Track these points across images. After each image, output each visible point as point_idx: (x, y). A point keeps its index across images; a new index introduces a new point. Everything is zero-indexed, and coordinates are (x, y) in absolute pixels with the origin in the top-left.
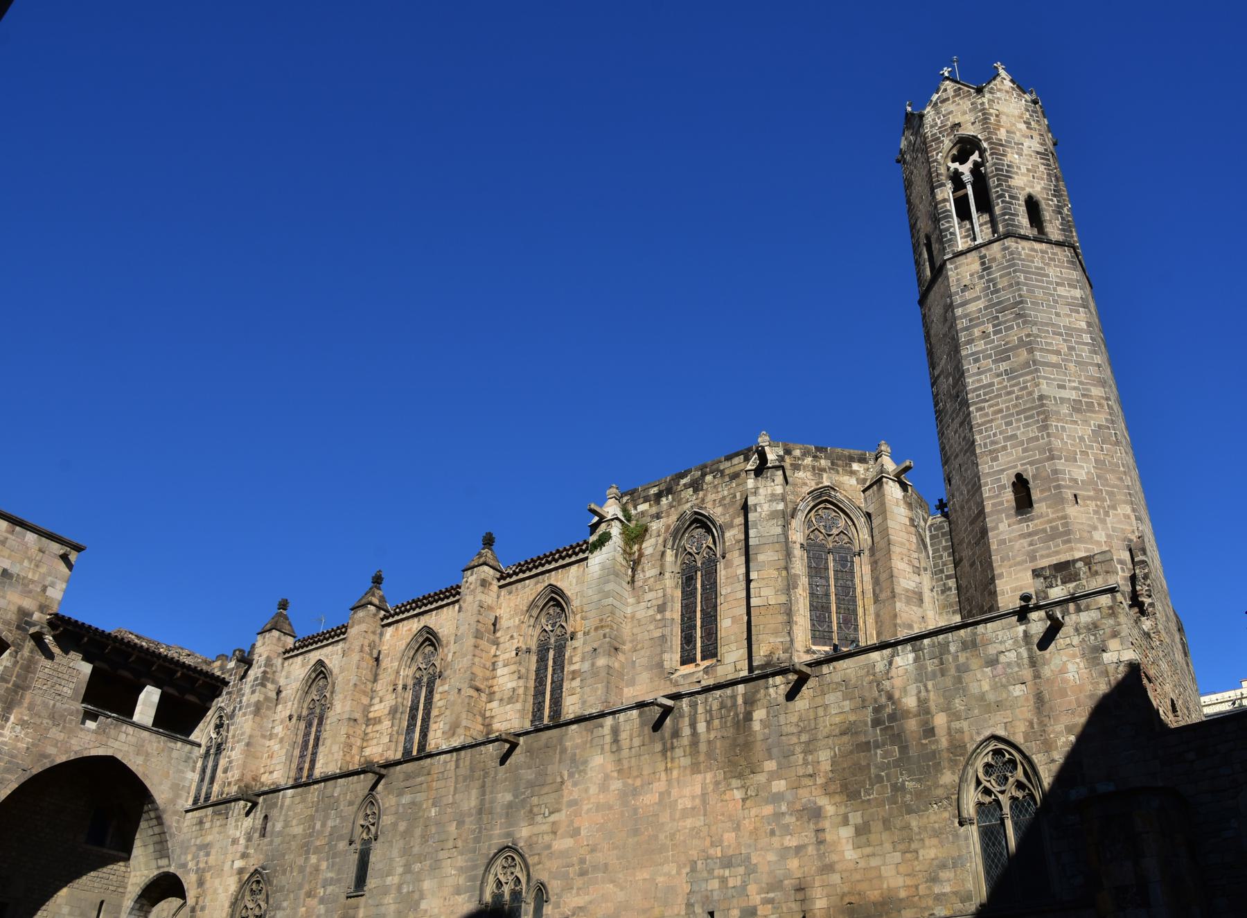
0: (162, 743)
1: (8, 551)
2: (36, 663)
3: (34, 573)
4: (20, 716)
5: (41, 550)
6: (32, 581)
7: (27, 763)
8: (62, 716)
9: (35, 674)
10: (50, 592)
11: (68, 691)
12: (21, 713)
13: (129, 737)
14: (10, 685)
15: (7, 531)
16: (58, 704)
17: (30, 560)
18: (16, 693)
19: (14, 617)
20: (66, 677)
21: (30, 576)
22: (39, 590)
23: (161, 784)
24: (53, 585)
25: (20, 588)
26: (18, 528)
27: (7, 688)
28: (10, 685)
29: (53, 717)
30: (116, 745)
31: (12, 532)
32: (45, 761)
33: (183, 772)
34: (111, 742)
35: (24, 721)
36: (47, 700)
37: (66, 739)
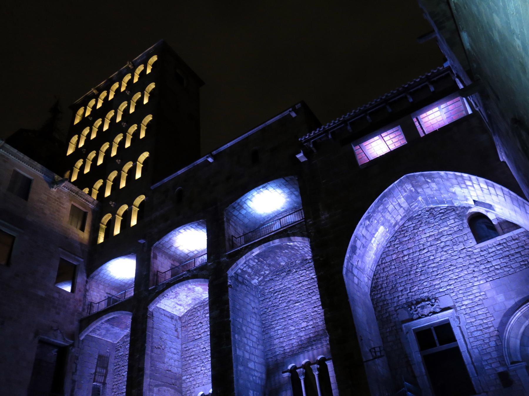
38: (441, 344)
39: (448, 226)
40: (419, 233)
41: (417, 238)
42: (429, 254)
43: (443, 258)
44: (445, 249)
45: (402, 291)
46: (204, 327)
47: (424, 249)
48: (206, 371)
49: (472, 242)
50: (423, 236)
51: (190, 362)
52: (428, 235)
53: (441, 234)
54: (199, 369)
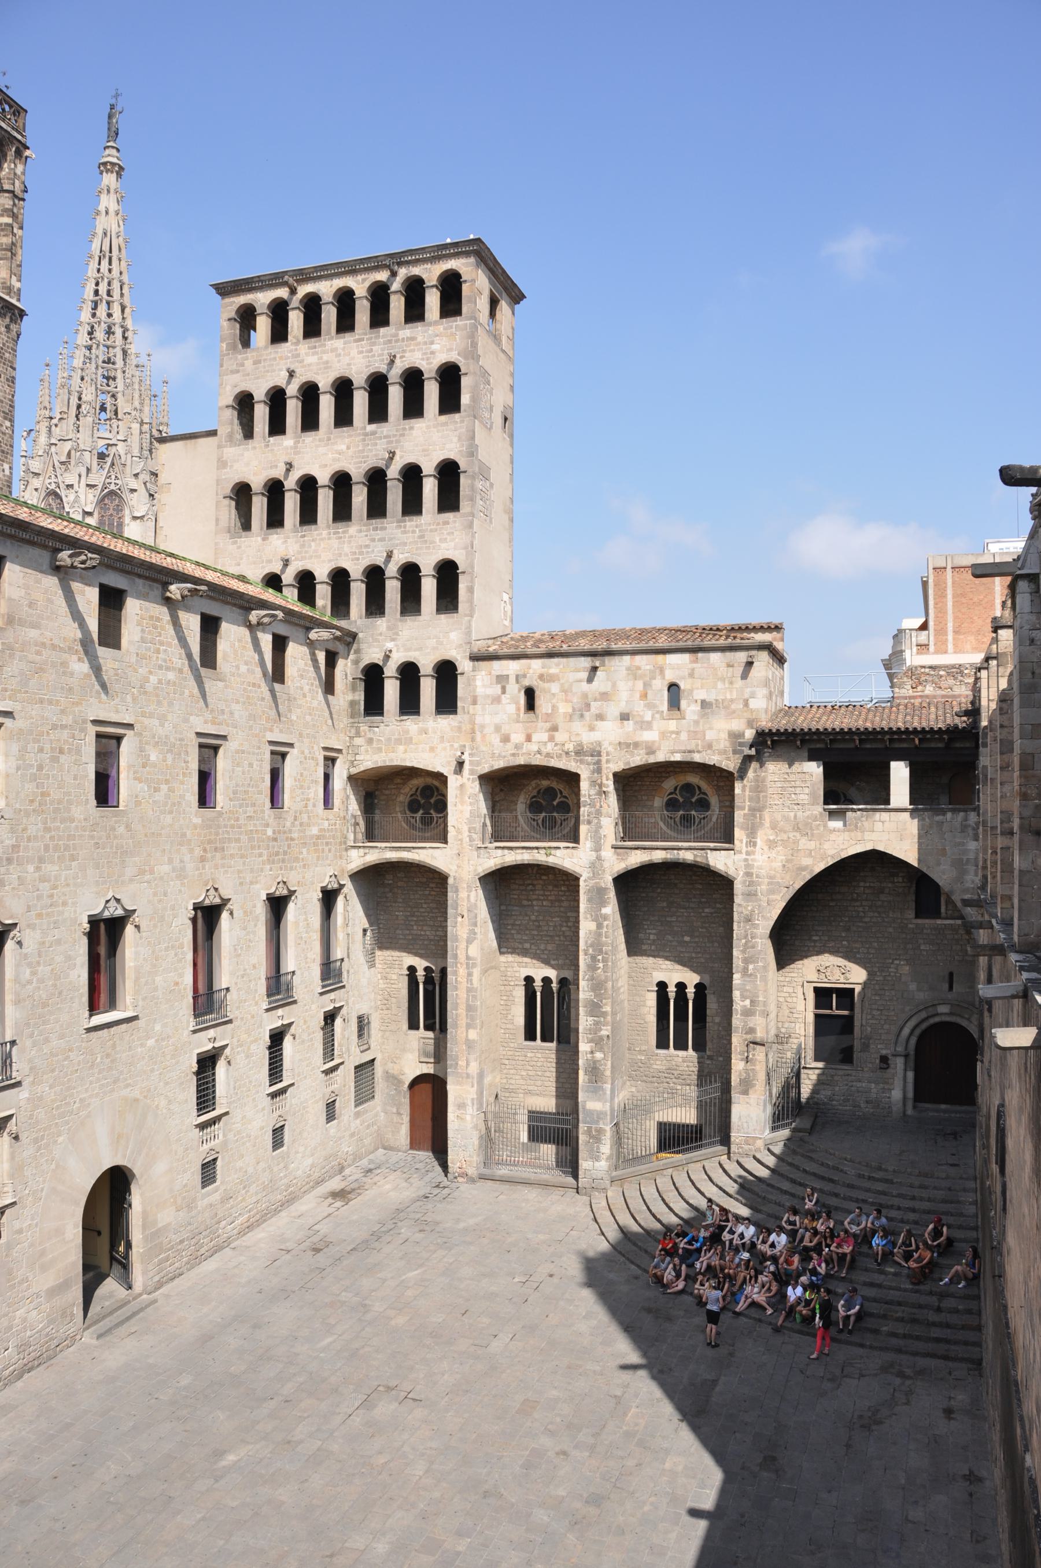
0: (927, 820)
1: (700, 680)
2: (763, 781)
3: (731, 692)
4: (766, 838)
5: (729, 666)
6: (732, 701)
7: (788, 880)
8: (806, 824)
9: (766, 792)
10: (753, 704)
11: (804, 798)
12: (766, 834)
13: (886, 824)
14: (746, 811)
15: (692, 662)
16: (800, 814)
17: (723, 680)
18: (754, 816)
19: (727, 744)
20: (798, 783)
21: (729, 697)
22: (742, 706)
23: (939, 864)
24: (753, 695)
25: (723, 712)
26: (700, 655)
27: (745, 815)
28: (746, 811)
29: (798, 828)
30: (874, 836)
31: (696, 661)
32: (804, 873)
33: (963, 844)
34: (868, 836)
35: (770, 841)
36: (785, 813)
37: (818, 846)
38: (837, 1009)
39: (893, 882)
40: (858, 878)
41: (854, 884)
42: (861, 909)
43: (874, 920)
44: (879, 910)
45: (815, 941)
46: (537, 892)
47: (857, 900)
48: (538, 952)
49: (911, 914)
50: (862, 884)
51: (513, 932)
52: (868, 885)
53: (881, 891)
54: (527, 946)
